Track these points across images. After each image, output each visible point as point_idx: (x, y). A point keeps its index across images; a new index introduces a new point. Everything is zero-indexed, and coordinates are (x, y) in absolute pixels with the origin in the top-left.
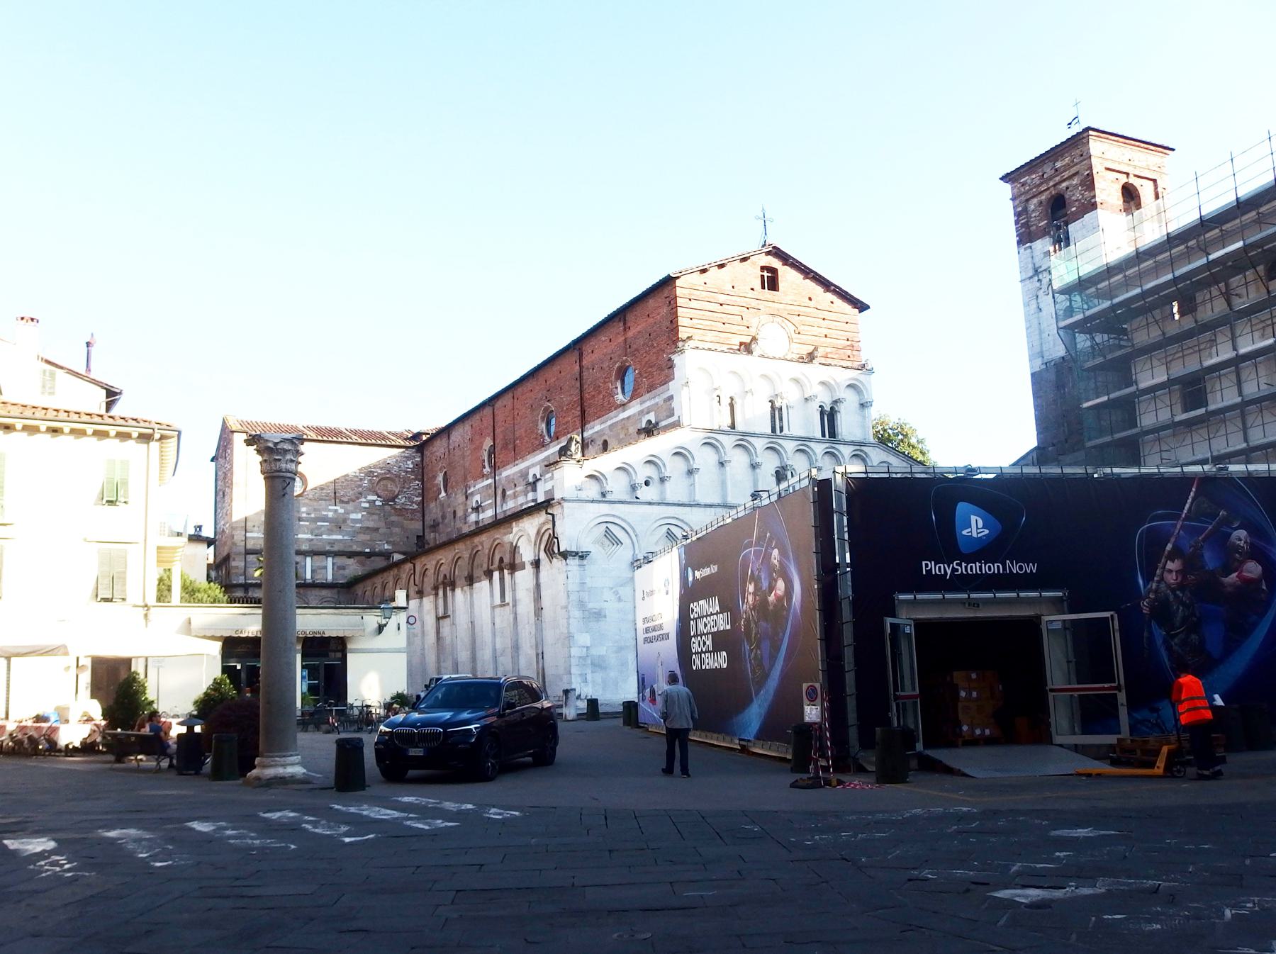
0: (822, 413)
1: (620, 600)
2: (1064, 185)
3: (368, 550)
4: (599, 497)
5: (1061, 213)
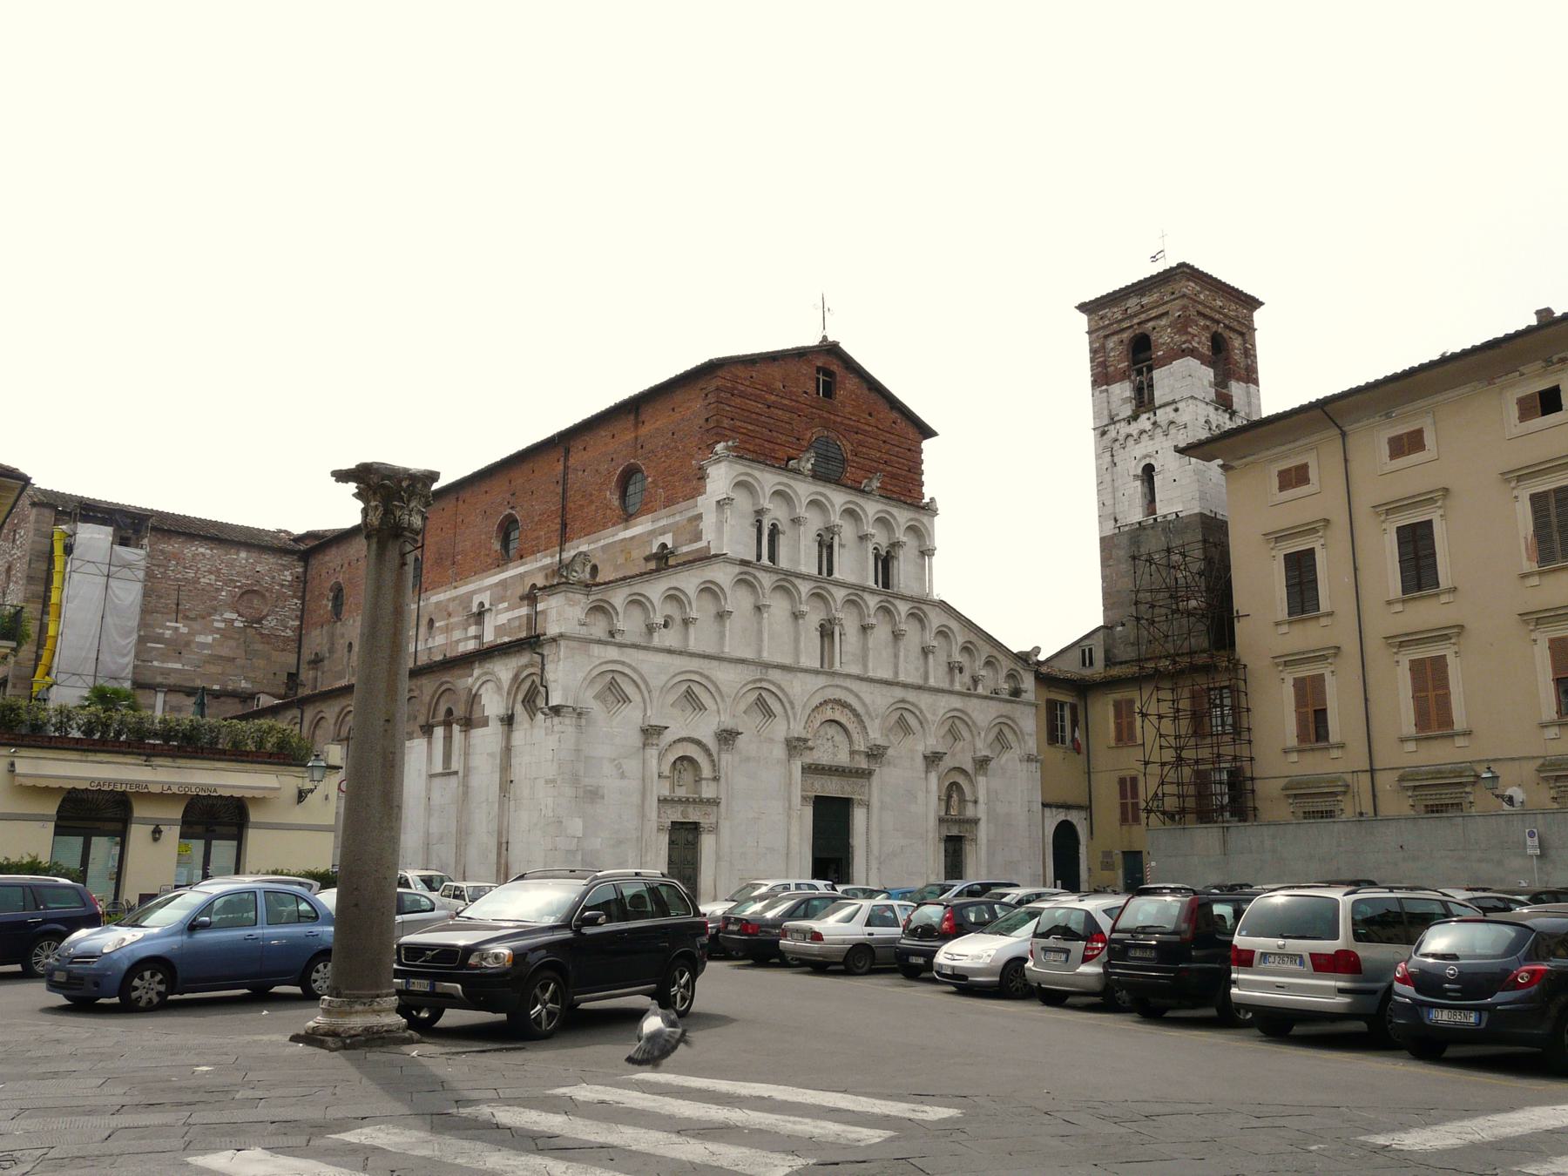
0: (877, 557)
1: (623, 776)
2: (1151, 324)
3: (216, 687)
4: (604, 636)
5: (1142, 356)
